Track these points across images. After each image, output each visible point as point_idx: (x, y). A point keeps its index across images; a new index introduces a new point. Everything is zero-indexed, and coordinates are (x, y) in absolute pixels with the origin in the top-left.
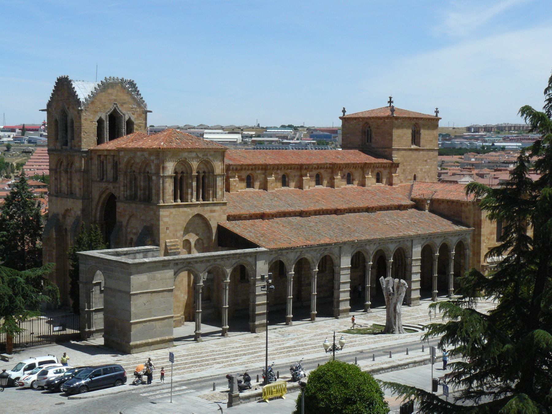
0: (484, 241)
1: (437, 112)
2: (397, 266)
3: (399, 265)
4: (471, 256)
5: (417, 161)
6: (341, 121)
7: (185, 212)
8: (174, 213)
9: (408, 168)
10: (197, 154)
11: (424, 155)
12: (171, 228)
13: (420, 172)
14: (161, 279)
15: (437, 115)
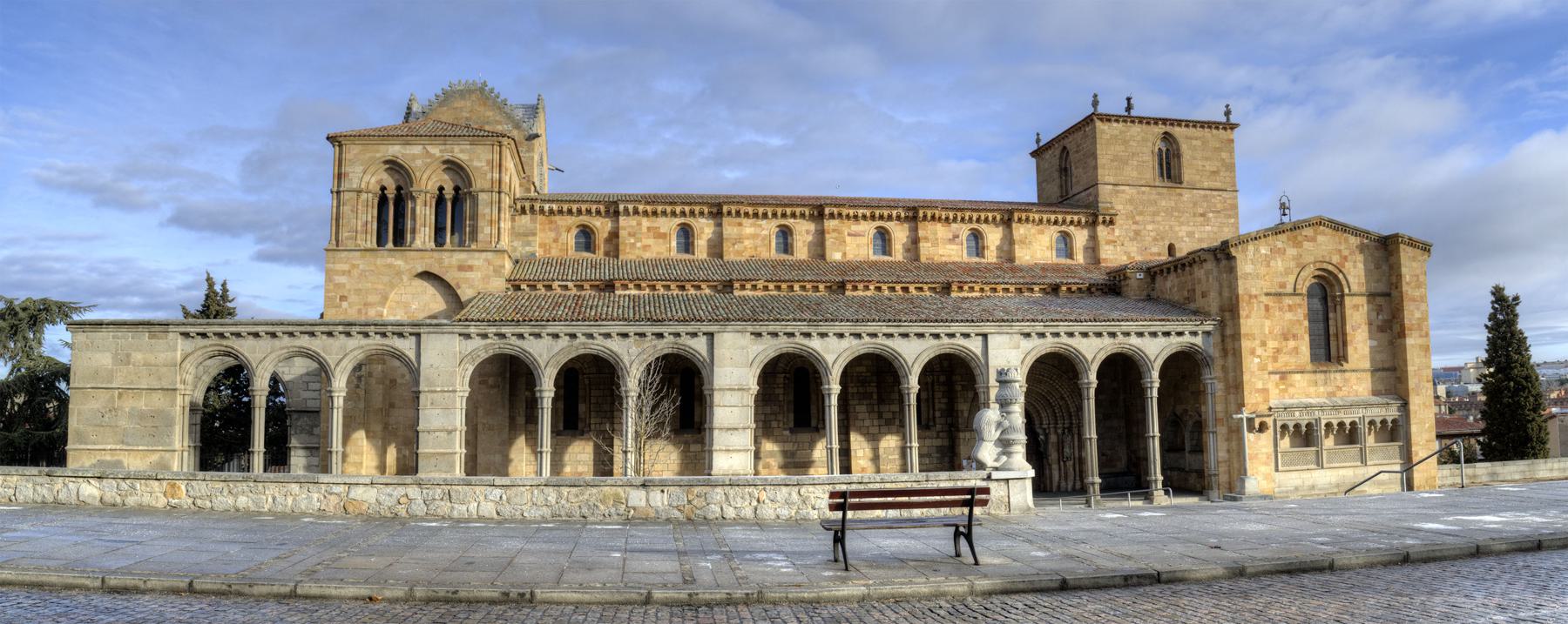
0: (1253, 352)
1: (1228, 113)
2: (1060, 431)
3: (1064, 428)
4: (1219, 393)
5: (1176, 214)
6: (1034, 160)
7: (390, 266)
8: (361, 267)
9: (1150, 227)
10: (425, 148)
11: (1195, 204)
12: (353, 298)
13: (1186, 239)
14: (144, 365)
15: (1228, 119)
